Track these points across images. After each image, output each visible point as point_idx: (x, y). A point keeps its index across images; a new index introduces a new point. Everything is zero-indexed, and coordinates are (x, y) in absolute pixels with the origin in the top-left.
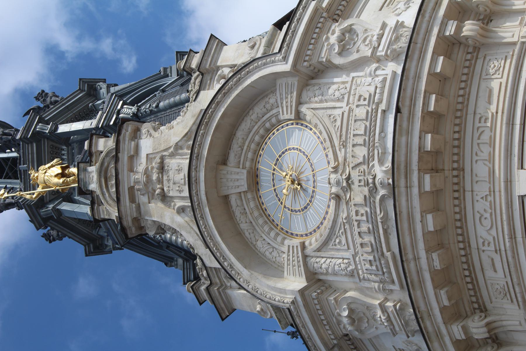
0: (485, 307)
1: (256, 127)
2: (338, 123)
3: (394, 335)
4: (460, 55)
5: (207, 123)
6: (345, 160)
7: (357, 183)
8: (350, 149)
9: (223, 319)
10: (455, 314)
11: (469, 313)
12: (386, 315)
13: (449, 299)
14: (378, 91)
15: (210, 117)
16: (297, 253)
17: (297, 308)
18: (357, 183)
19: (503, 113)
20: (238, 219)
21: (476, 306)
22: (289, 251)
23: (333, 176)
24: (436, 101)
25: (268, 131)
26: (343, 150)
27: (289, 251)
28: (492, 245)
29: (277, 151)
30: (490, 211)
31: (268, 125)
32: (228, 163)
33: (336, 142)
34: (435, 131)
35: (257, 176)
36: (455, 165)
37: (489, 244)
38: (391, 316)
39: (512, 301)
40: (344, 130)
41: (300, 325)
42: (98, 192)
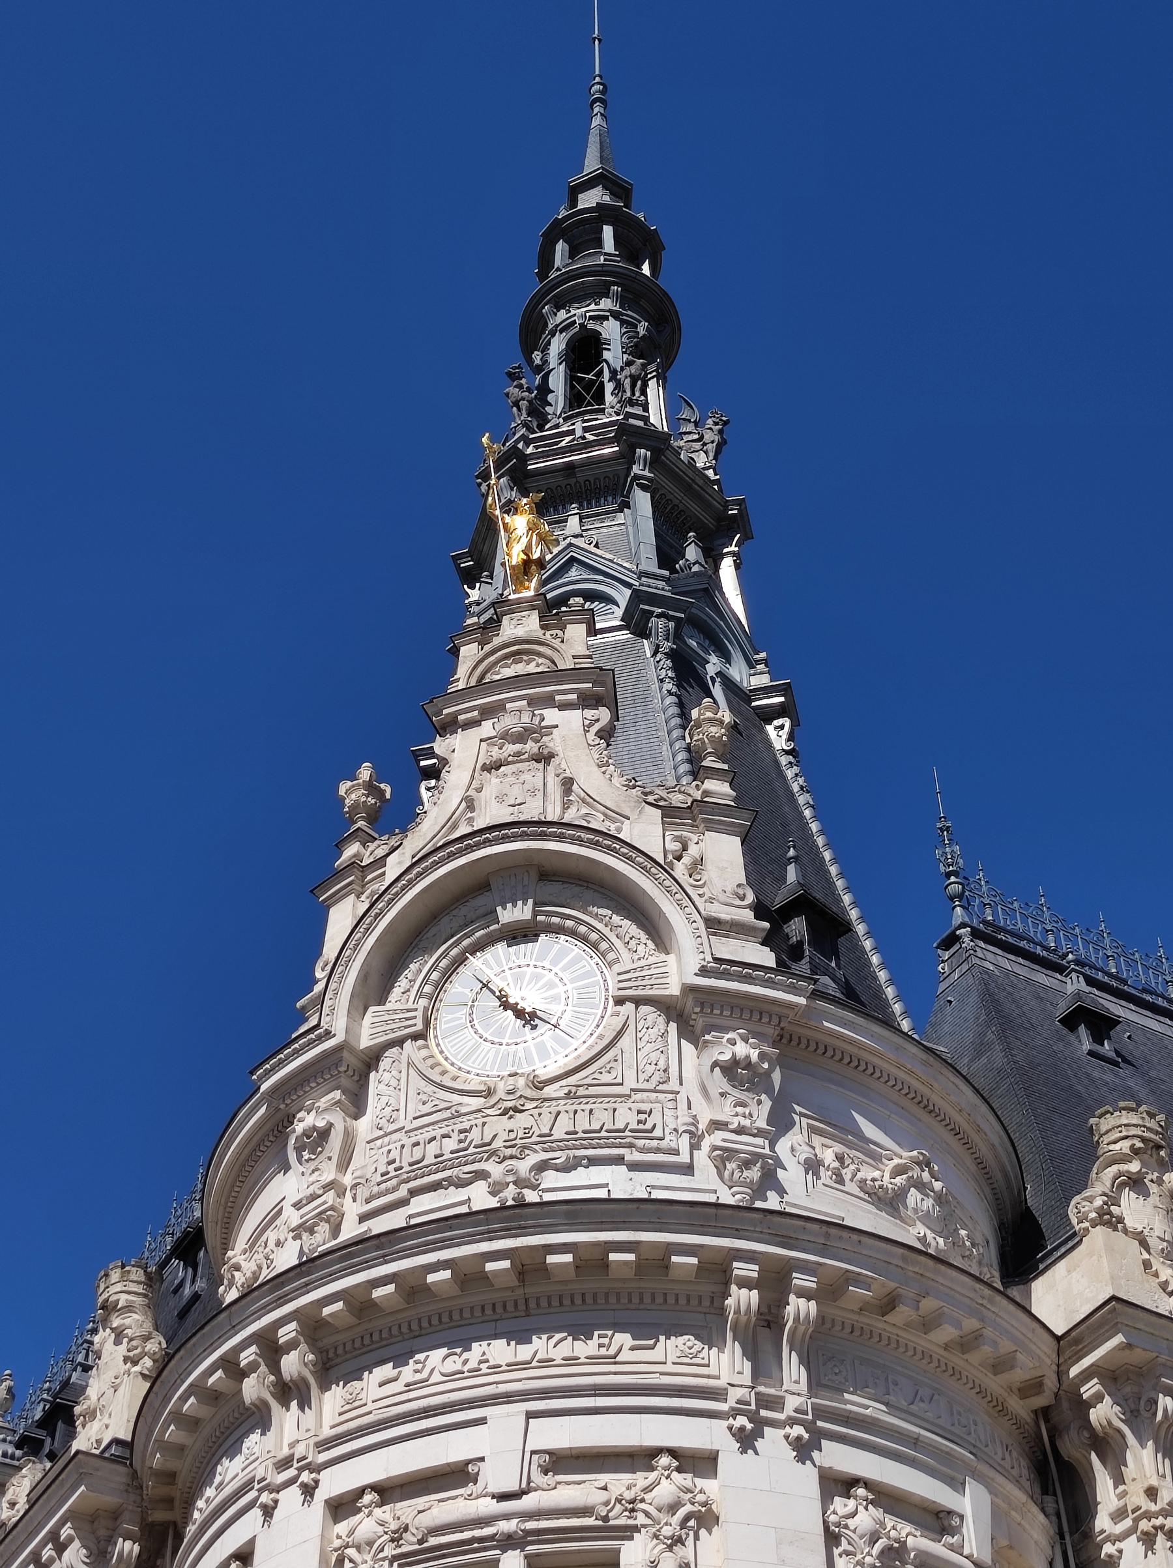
0: (332, 1367)
1: (599, 926)
2: (606, 1078)
3: (294, 1205)
4: (706, 1288)
5: (597, 843)
6: (545, 1100)
7: (511, 1125)
8: (561, 1106)
9: (311, 891)
10: (313, 1327)
11: (320, 1344)
12: (320, 1192)
13: (330, 1315)
14: (655, 1143)
15: (608, 847)
16: (406, 1027)
17: (320, 1039)
18: (511, 1125)
19: (615, 1373)
20: (454, 913)
21: (331, 1355)
22: (408, 1011)
23: (521, 1082)
24: (626, 1263)
25: (595, 946)
26: (561, 1094)
27: (408, 1011)
28: (418, 1377)
29: (564, 969)
30: (466, 1368)
31: (604, 946)
32: (541, 884)
33: (572, 1080)
34: (579, 1266)
35: (525, 936)
36: (532, 1304)
37: (416, 1371)
38: (319, 1201)
39: (340, 1415)
40: (593, 1091)
41: (296, 1045)
42: (496, 641)
